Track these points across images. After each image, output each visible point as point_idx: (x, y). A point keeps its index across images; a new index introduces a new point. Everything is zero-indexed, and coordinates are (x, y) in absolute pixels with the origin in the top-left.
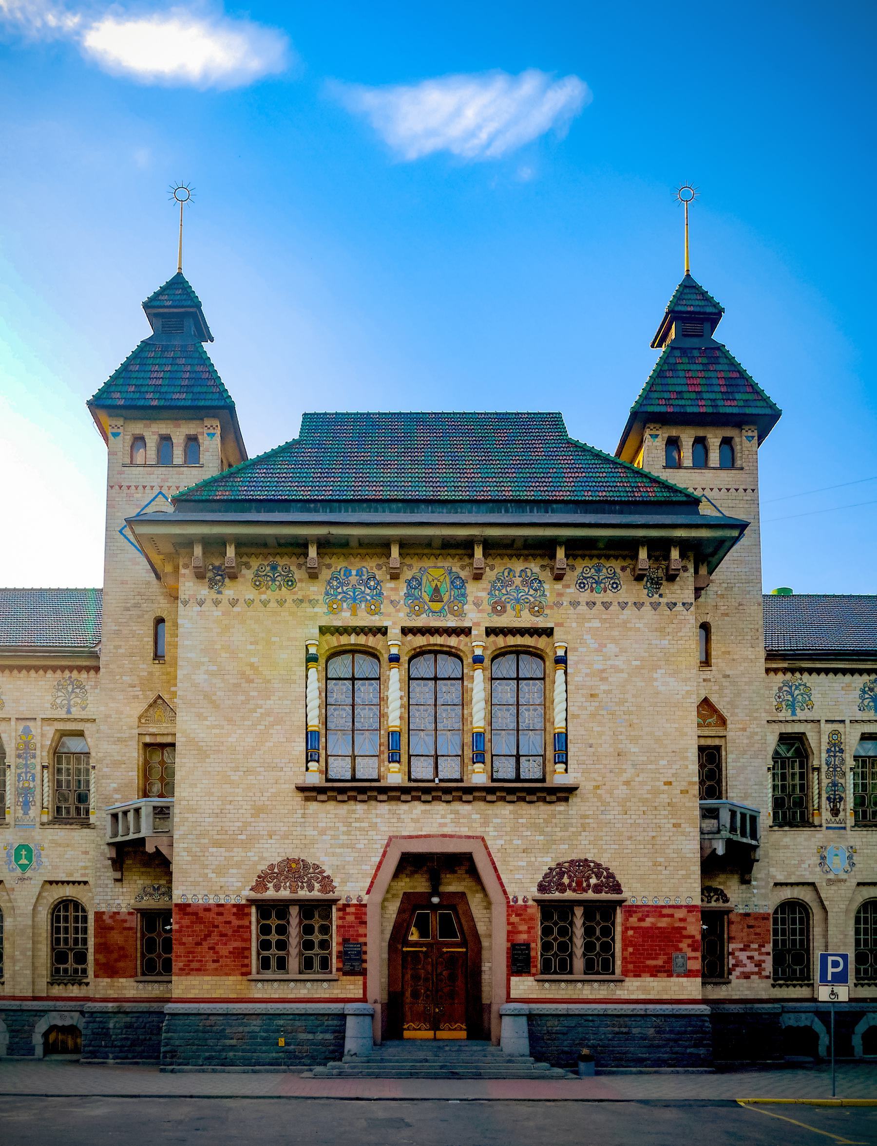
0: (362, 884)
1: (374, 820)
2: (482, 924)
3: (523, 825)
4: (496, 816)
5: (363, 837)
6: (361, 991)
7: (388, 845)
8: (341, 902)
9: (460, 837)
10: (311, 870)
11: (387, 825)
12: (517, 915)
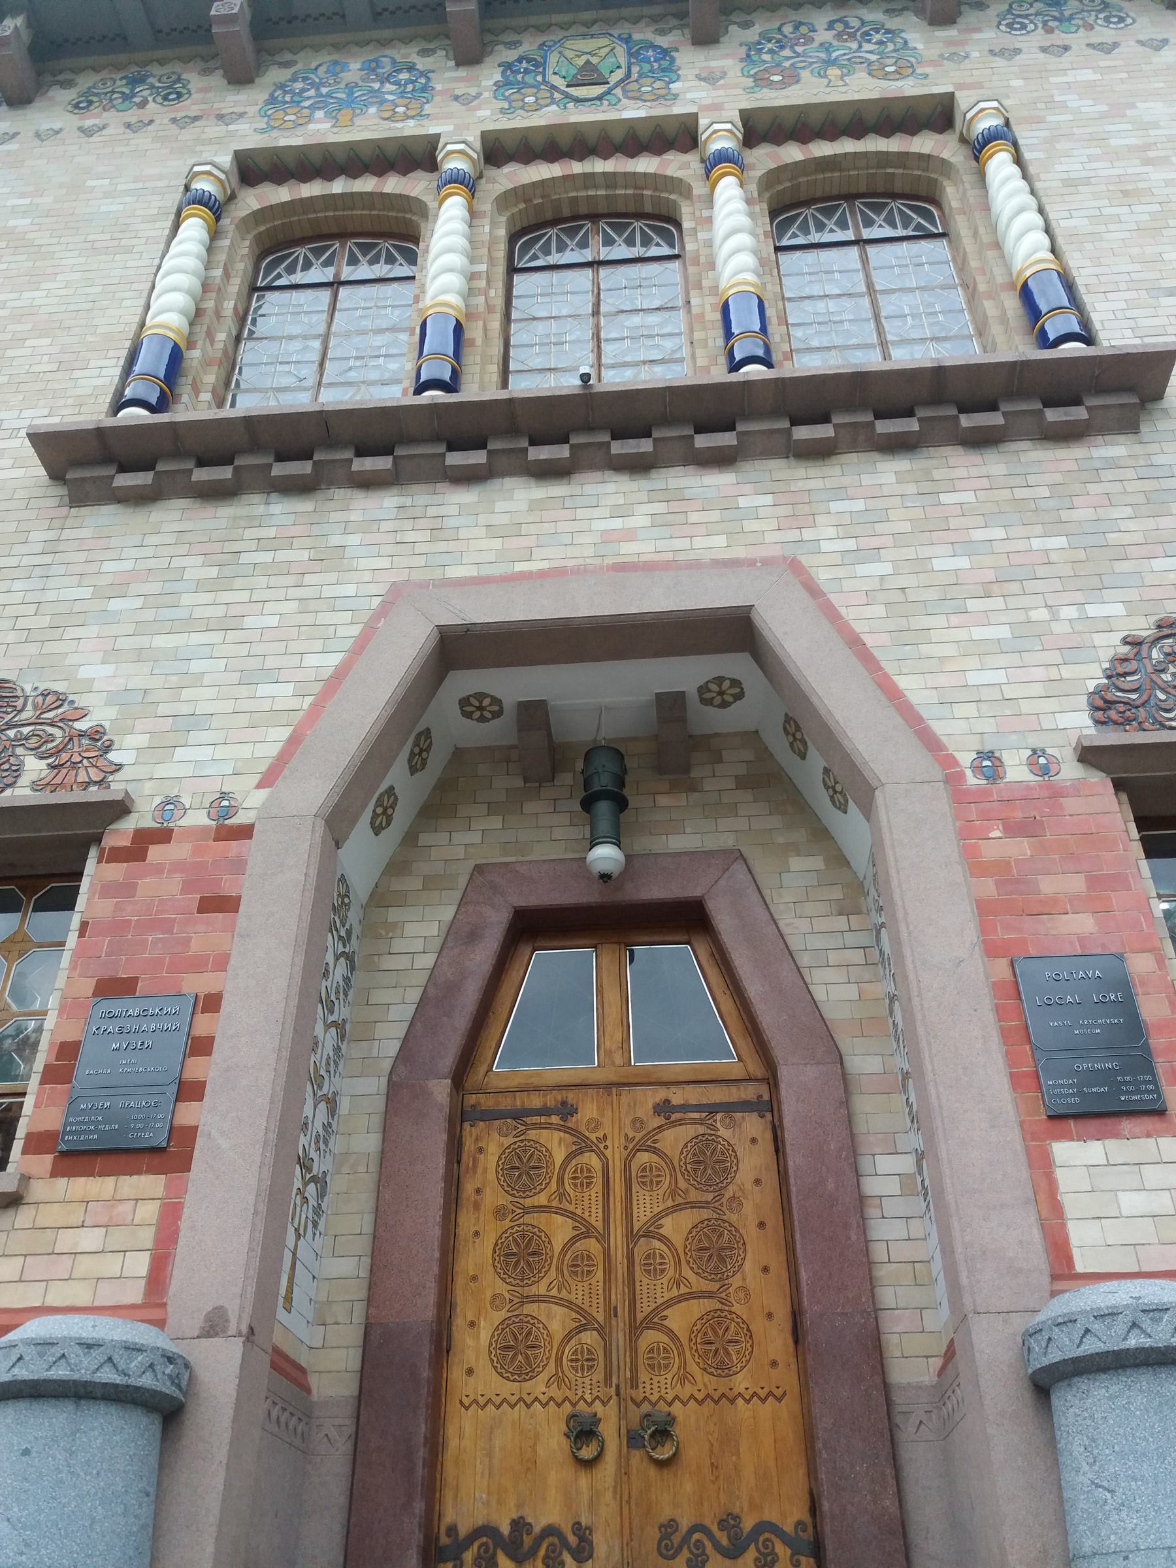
0: (246, 751)
1: (335, 541)
2: (829, 975)
3: (964, 510)
4: (841, 492)
5: (281, 594)
6: (140, 1264)
7: (383, 611)
8: (129, 824)
9: (695, 565)
10: (28, 713)
11: (389, 549)
12: (1014, 829)
